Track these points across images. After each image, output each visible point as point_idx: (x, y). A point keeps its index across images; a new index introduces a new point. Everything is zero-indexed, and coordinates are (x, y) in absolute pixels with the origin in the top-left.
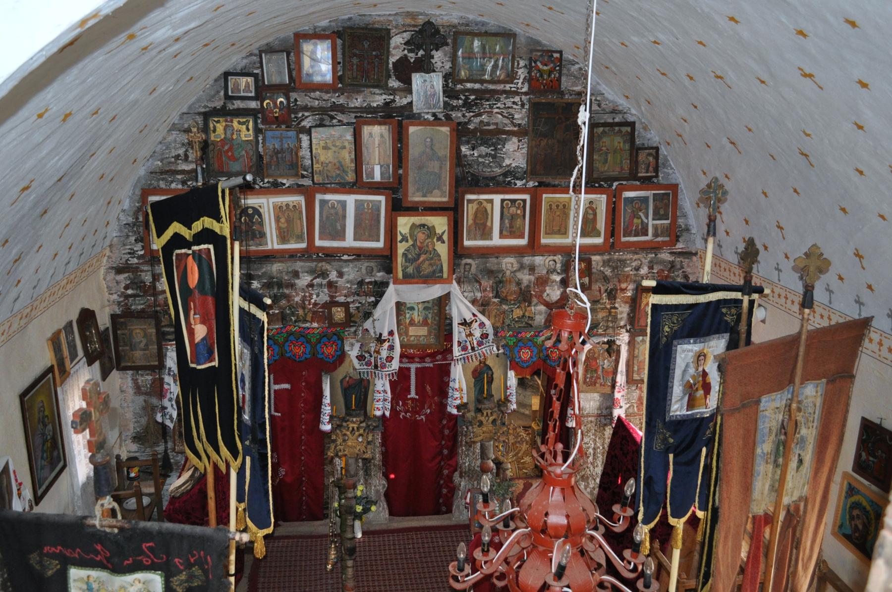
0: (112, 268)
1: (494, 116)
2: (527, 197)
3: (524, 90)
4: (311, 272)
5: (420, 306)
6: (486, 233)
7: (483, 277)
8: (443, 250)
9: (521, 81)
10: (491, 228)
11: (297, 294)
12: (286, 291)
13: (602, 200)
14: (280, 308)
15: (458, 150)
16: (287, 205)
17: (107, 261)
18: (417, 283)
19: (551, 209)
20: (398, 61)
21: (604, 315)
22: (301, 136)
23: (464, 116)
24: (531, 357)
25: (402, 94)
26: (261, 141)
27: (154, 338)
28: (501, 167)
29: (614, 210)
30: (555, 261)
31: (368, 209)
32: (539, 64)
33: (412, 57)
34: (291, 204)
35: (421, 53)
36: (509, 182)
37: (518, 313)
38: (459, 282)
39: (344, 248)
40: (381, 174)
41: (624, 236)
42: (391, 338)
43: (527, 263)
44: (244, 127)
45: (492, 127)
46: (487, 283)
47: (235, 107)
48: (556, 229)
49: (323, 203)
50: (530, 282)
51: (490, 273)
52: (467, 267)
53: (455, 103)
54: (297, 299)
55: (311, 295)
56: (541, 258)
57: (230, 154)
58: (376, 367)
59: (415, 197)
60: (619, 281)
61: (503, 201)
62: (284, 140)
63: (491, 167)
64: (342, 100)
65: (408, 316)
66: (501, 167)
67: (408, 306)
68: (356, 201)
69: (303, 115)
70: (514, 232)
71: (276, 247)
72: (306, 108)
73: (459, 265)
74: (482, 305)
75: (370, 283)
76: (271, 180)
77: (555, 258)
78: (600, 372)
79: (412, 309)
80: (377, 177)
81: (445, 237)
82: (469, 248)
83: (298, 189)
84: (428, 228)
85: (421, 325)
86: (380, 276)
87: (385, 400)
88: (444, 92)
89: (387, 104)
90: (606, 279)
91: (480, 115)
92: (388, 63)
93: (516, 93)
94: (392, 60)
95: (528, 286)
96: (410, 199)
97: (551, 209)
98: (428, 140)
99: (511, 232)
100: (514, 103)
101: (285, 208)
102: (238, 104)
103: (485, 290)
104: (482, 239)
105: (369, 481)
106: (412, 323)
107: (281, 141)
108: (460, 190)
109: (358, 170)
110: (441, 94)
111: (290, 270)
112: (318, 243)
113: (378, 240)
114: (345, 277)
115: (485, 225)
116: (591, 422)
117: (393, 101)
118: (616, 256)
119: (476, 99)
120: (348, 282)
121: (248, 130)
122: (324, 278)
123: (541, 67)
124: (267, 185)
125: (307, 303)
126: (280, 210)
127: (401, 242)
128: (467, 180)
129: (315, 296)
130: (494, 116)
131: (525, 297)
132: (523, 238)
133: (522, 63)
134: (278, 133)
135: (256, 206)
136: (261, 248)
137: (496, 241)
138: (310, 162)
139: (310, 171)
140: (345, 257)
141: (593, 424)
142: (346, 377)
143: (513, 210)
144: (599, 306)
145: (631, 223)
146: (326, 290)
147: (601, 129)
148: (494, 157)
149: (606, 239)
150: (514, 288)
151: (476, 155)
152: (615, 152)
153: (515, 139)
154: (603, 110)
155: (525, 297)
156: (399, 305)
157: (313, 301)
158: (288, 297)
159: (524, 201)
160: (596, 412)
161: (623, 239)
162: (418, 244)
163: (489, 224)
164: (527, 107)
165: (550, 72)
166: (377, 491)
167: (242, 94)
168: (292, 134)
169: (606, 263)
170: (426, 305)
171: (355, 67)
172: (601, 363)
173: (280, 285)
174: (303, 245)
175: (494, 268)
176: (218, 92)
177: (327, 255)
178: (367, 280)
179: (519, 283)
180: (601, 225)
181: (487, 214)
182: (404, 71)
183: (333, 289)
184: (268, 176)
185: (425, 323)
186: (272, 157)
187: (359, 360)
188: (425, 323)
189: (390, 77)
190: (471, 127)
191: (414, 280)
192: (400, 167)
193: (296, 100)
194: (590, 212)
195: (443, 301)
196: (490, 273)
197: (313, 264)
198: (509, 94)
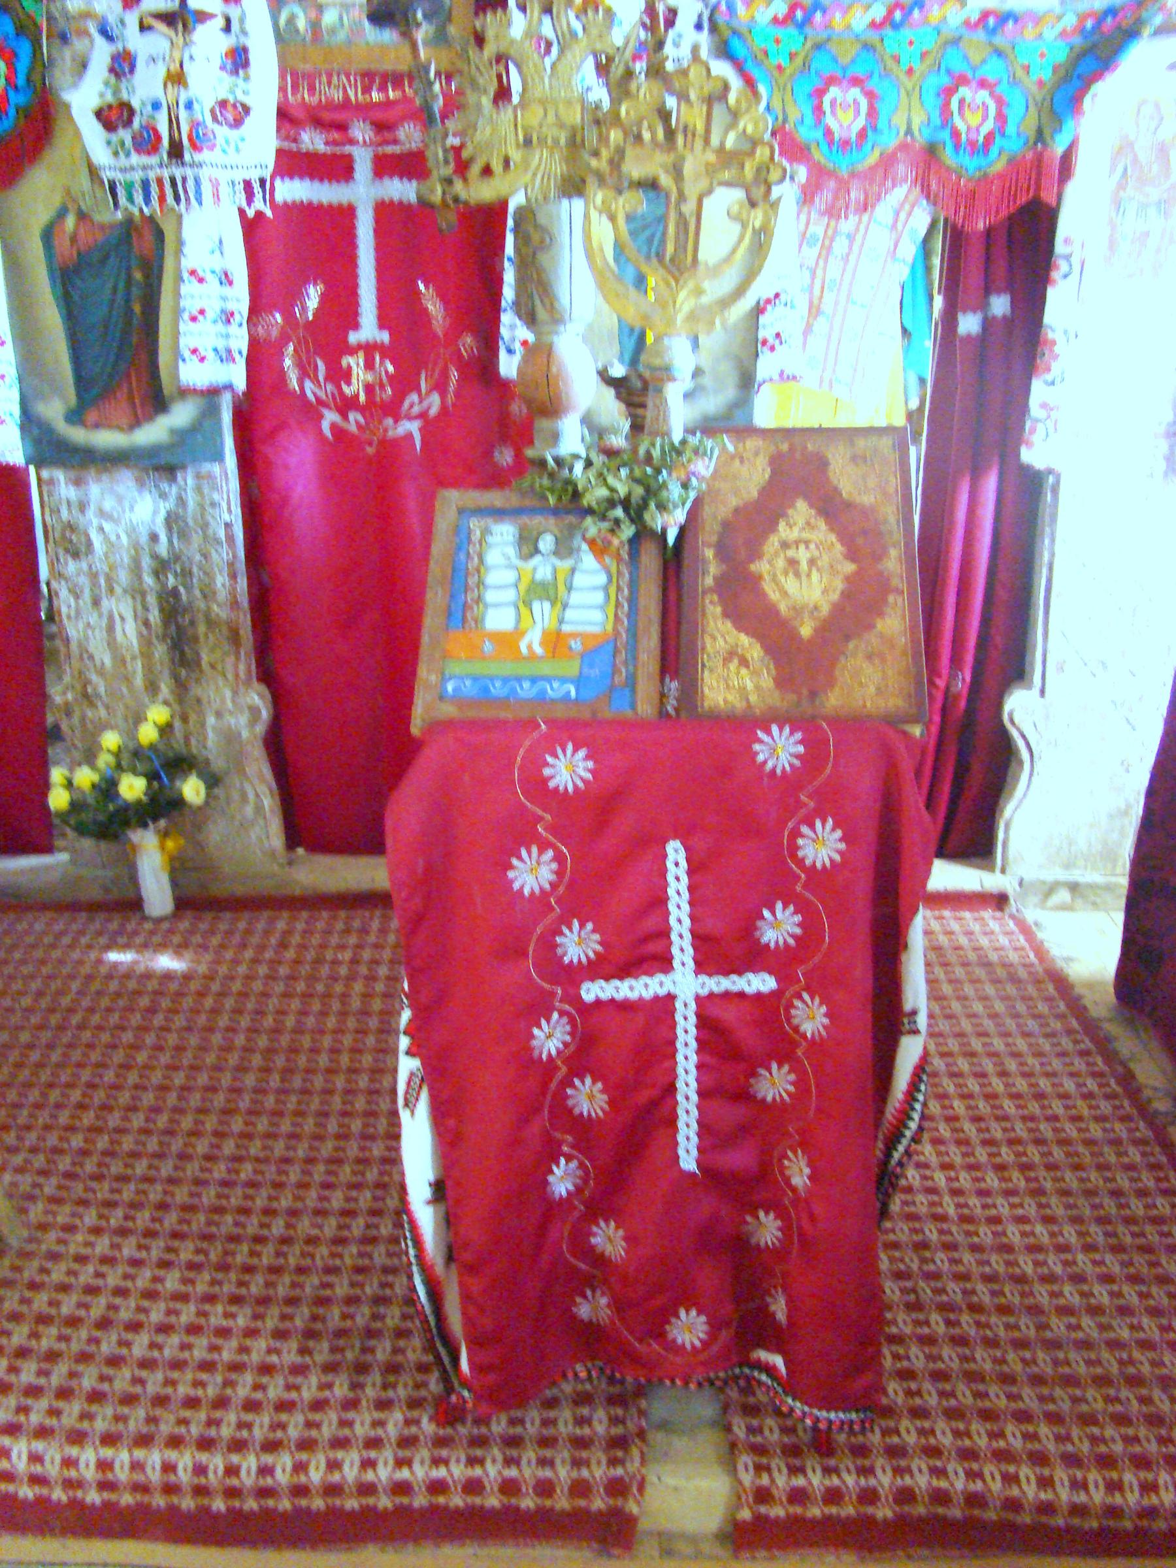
105: (196, 690)
142: (62, 214)
187: (109, 126)
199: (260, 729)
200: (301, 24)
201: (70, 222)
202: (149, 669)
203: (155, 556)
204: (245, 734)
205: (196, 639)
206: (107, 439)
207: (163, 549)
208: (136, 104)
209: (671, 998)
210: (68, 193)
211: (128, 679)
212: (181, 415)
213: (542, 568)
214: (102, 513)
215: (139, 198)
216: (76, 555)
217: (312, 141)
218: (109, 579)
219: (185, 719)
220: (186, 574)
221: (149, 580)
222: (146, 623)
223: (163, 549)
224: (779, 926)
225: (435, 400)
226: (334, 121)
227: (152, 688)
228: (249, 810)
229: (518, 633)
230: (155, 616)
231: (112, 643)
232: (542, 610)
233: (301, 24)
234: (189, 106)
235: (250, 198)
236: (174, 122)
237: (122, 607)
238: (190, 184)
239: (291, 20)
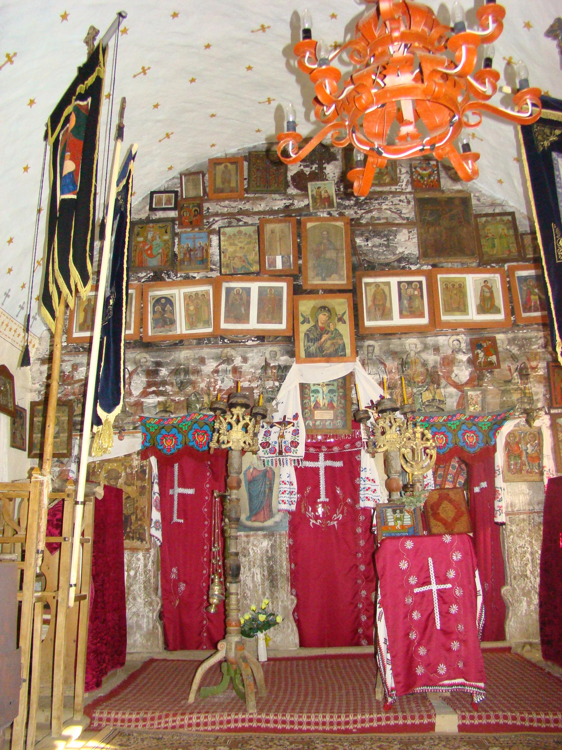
0: (39, 359)
1: (385, 210)
2: (423, 279)
3: (408, 190)
4: (218, 358)
5: (326, 389)
6: (386, 313)
7: (387, 358)
8: (345, 330)
9: (404, 183)
10: (391, 310)
11: (203, 381)
12: (193, 378)
13: (496, 279)
14: (186, 395)
15: (353, 242)
16: (197, 294)
17: (36, 352)
18: (320, 361)
19: (447, 288)
20: (295, 174)
21: (519, 396)
22: (211, 236)
23: (356, 213)
24: (447, 442)
25: (301, 198)
26: (176, 243)
27: (66, 426)
28: (394, 254)
29: (509, 289)
30: (458, 340)
31: (271, 294)
32: (418, 169)
33: (307, 171)
34: (200, 294)
35: (315, 166)
36: (404, 268)
37: (427, 396)
38: (363, 364)
39: (248, 330)
40: (283, 263)
41: (524, 312)
42: (295, 422)
43: (431, 343)
44: (164, 230)
45: (382, 221)
46: (392, 364)
47: (158, 217)
48: (454, 306)
49: (228, 290)
50: (436, 363)
51: (394, 354)
52: (371, 349)
53: (347, 203)
54: (203, 385)
55: (216, 381)
56: (444, 338)
57: (149, 252)
58: (281, 453)
59: (314, 280)
60: (528, 360)
61: (399, 283)
62: (197, 240)
63: (385, 255)
64: (248, 206)
65: (312, 399)
66: (394, 254)
67: (313, 388)
68: (259, 287)
69: (214, 220)
70: (414, 312)
71: (185, 332)
72: (217, 214)
73: (361, 347)
74: (389, 388)
75: (274, 367)
76: (183, 275)
77: (458, 337)
78: (524, 458)
79: (317, 391)
80: (279, 265)
81: (346, 318)
82: (369, 328)
83: (207, 280)
84: (329, 310)
85: (327, 409)
86: (283, 360)
87: (291, 493)
88: (337, 195)
89: (287, 207)
90: (514, 358)
91: (370, 211)
92: (286, 177)
93: (401, 193)
94: (290, 174)
95: (434, 367)
96: (309, 283)
97: (447, 288)
98: (325, 233)
99: (410, 312)
100: (400, 201)
101: (194, 297)
102: (160, 215)
103: (390, 372)
104: (382, 319)
105: (276, 594)
106: (317, 406)
107: (194, 241)
108: (357, 273)
109: (261, 262)
110: (334, 196)
111: (197, 356)
112: (224, 326)
113: (281, 323)
114: (250, 362)
115: (384, 305)
116: (524, 520)
117: (292, 204)
118: (521, 334)
119: (366, 199)
120: (252, 367)
121: (166, 232)
122: (229, 364)
123: (420, 171)
124: (179, 279)
125: (212, 389)
126: (189, 298)
127: (303, 323)
128: (362, 266)
129: (219, 382)
130: (385, 210)
131: (433, 378)
132: (424, 317)
133: (404, 170)
134: (191, 235)
135: (169, 297)
136: (170, 333)
137: (397, 321)
138: (218, 257)
139: (218, 265)
140: (250, 343)
141: (526, 523)
142: (249, 468)
143: (410, 291)
144: (512, 387)
145: (529, 300)
146: (230, 376)
147: (484, 219)
148: (387, 246)
149: (506, 315)
150: (420, 369)
151: (370, 245)
152: (501, 237)
153: (405, 231)
154: (483, 204)
155: (433, 378)
156: (303, 387)
157: (217, 387)
158: (193, 384)
159: (420, 283)
160: (527, 508)
161: (524, 315)
162: (320, 324)
163: (388, 304)
164: (412, 203)
165: (430, 175)
166: (285, 608)
167: (164, 206)
168: (204, 235)
169: (511, 341)
170: (331, 387)
171: (258, 179)
172: (524, 448)
173: (187, 372)
174: (210, 330)
175: (398, 349)
176: (145, 207)
177: (232, 341)
178: (272, 365)
179: (424, 364)
180: (500, 301)
181: (385, 296)
182: (301, 181)
183: (238, 375)
184: (181, 270)
185: (331, 406)
186: (185, 254)
187: (264, 447)
188: (331, 406)
189: (289, 186)
190: (363, 221)
191: (317, 359)
192: (300, 258)
193: (208, 209)
194: (486, 290)
195: (347, 383)
196: (394, 354)
197: (219, 351)
198: (394, 194)
199: (294, 606)
200: (311, 424)
201: (251, 470)
202: (263, 588)
203: (267, 557)
204: (290, 607)
205: (277, 580)
206: (257, 524)
207: (269, 555)
208: (270, 442)
209: (432, 590)
210: (251, 462)
211: (257, 591)
212: (278, 518)
213: (398, 515)
214: (254, 545)
215: (270, 464)
216: (245, 556)
217: (312, 450)
218: (254, 563)
219: (272, 603)
220: (275, 562)
221: (265, 563)
222: (264, 575)
223: (269, 555)
224: (451, 574)
225: (340, 516)
226: (318, 446)
227: (264, 594)
228: (290, 631)
229: (395, 526)
230: (266, 573)
231: (253, 581)
232: (399, 522)
233: (311, 424)
234: (285, 442)
235: (299, 464)
236: (280, 446)
237: (257, 571)
238: (285, 461)
239: (308, 424)
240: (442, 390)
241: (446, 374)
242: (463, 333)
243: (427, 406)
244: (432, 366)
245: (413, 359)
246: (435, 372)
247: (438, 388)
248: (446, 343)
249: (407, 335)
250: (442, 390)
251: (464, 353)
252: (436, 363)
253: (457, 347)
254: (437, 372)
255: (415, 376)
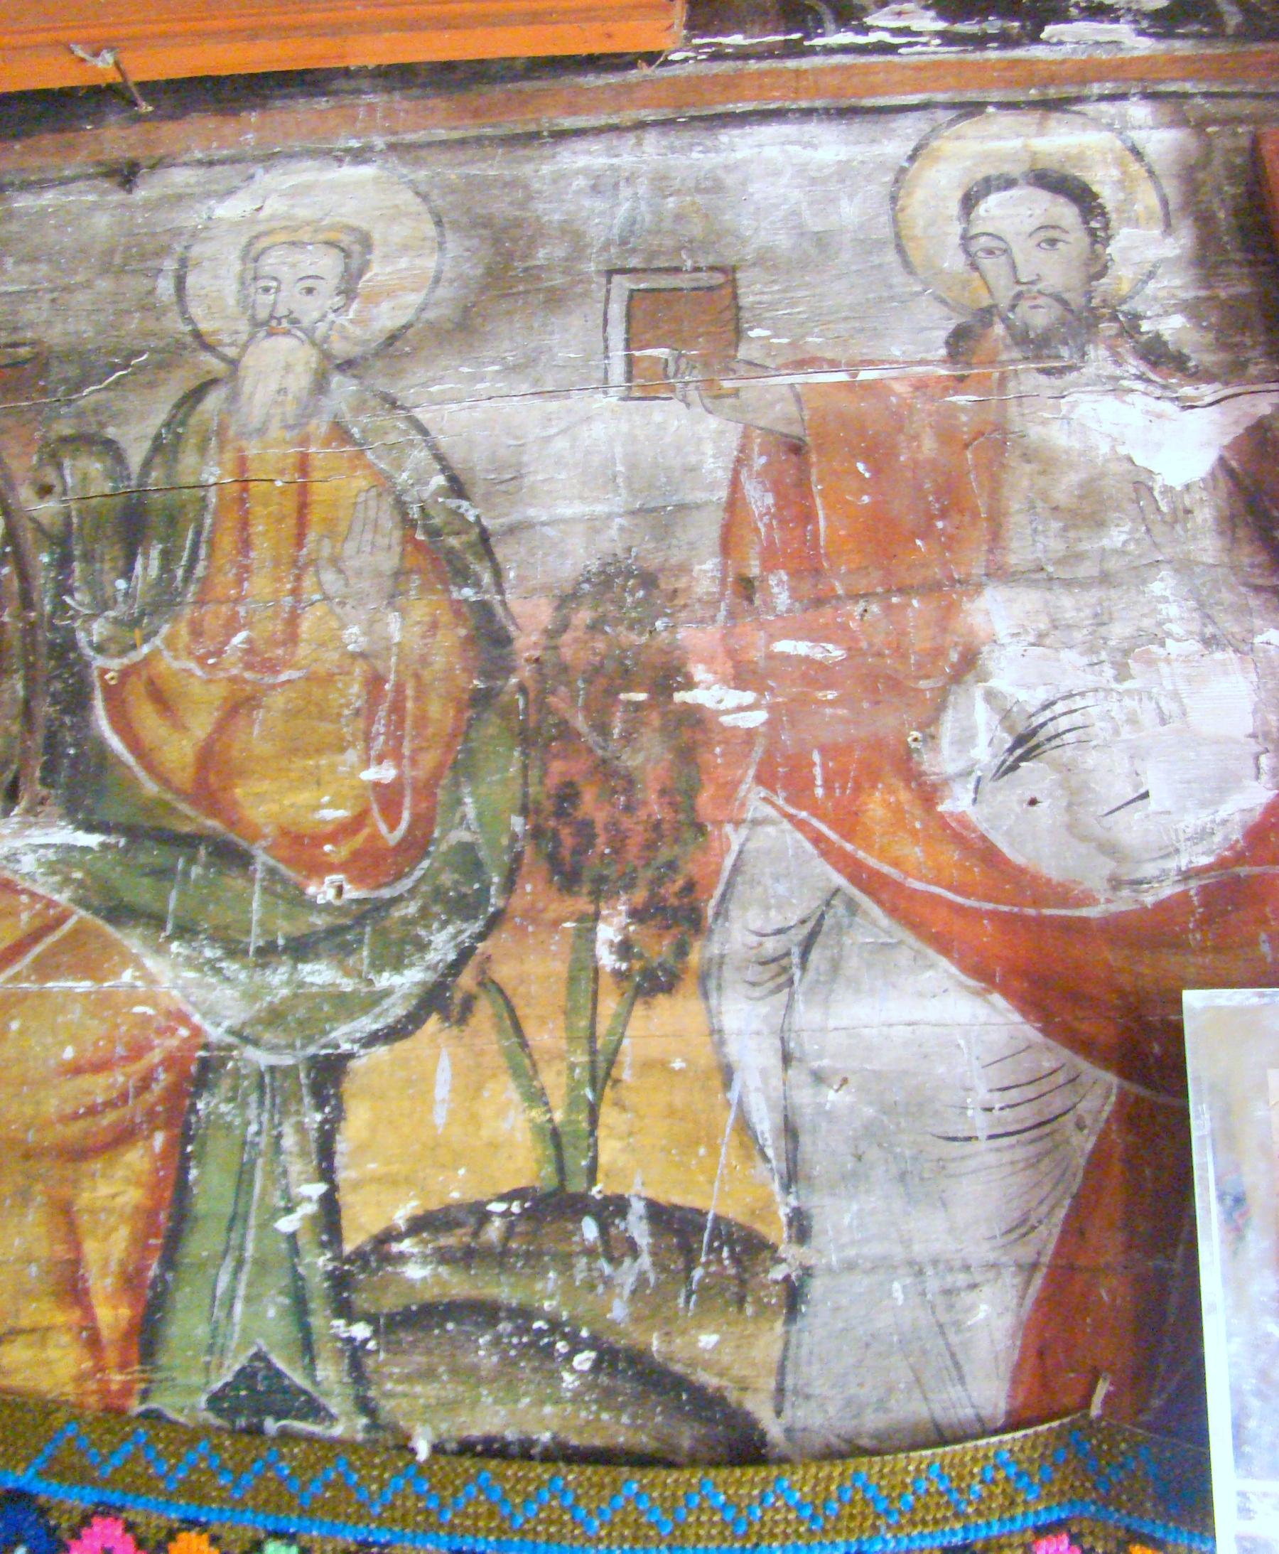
37: (437, 1127)
43: (604, 219)
50: (660, 517)
56: (830, 145)
77: (1060, 140)
95: (631, 584)
150: (367, 619)
175: (65, 322)
179: (451, 544)
240: (743, 1018)
241: (832, 714)
242: (1127, 80)
243: (424, 1316)
244: (576, 558)
245: (270, 455)
246: (611, 677)
247: (652, 983)
248: (853, 211)
249: (250, 129)
250: (743, 1018)
251: (1160, 357)
252: (660, 517)
253: (1055, 271)
254: (668, 676)
255: (256, 736)
